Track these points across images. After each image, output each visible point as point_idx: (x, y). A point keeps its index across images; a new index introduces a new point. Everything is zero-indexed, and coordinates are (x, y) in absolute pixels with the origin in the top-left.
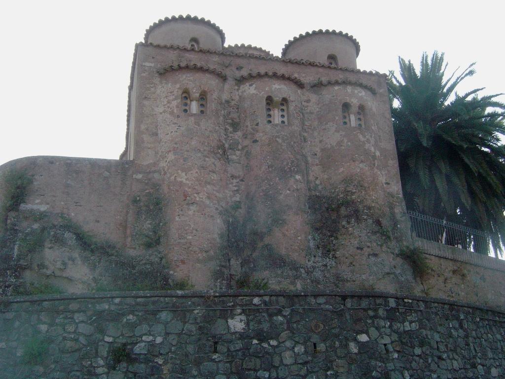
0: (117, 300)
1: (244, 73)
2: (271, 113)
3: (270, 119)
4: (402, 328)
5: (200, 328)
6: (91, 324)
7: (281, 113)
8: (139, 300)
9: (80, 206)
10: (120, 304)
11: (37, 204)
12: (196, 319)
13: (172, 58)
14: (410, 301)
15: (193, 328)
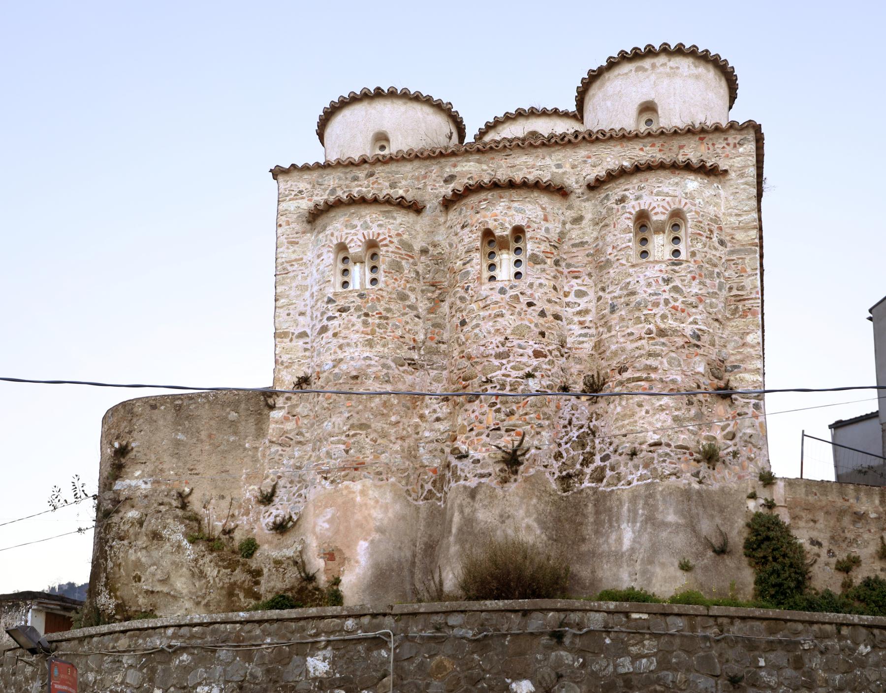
0: (170, 631)
1: (458, 185)
2: (496, 260)
3: (492, 273)
4: (611, 668)
5: (268, 671)
6: (141, 669)
7: (514, 257)
8: (195, 629)
9: (197, 474)
10: (175, 636)
11: (137, 478)
12: (262, 657)
13: (335, 185)
14: (645, 616)
15: (259, 672)
